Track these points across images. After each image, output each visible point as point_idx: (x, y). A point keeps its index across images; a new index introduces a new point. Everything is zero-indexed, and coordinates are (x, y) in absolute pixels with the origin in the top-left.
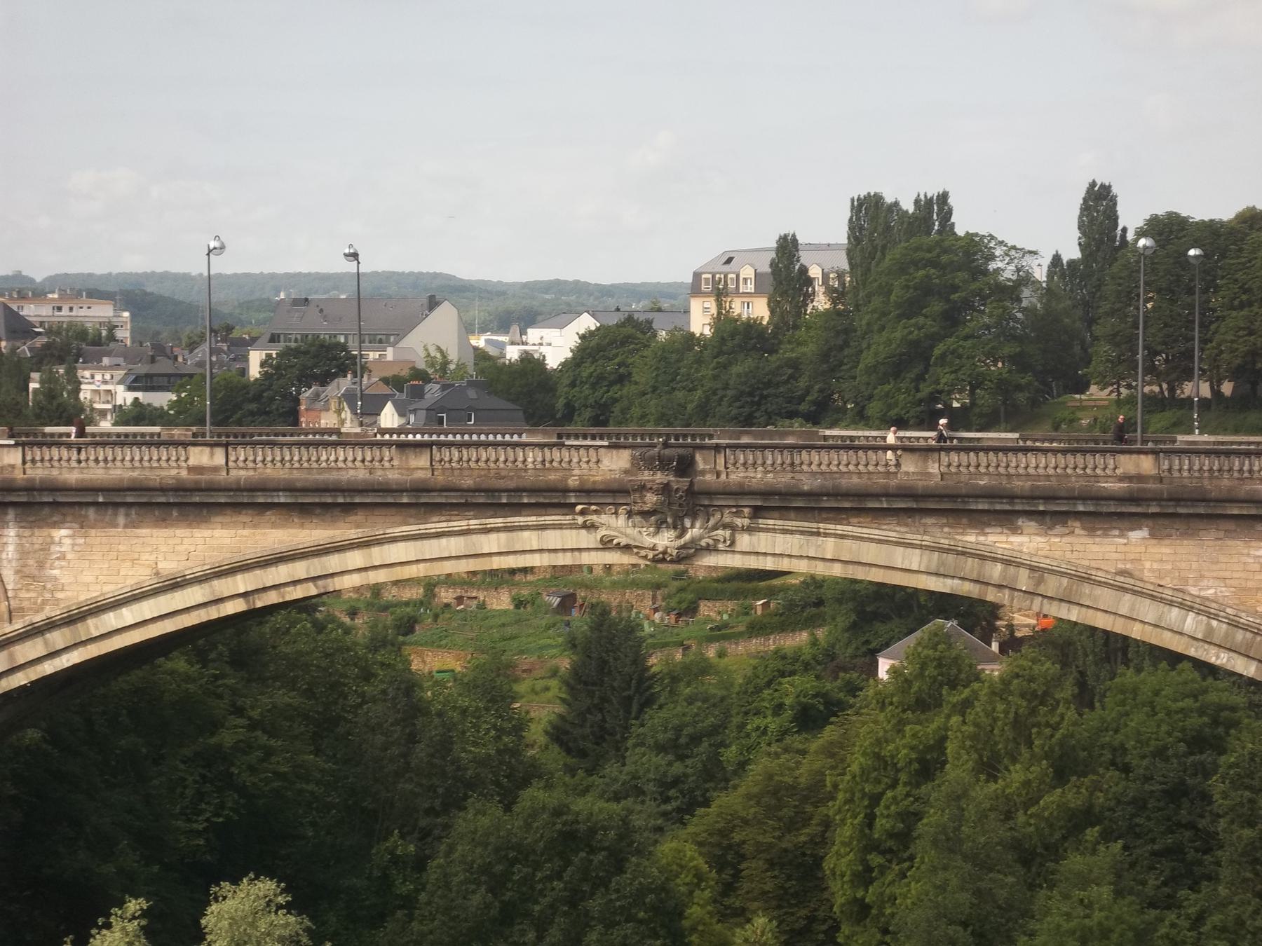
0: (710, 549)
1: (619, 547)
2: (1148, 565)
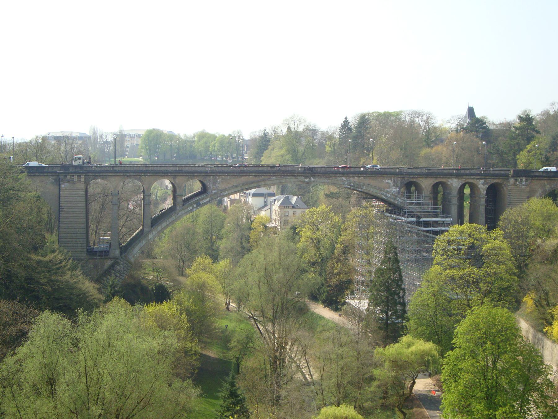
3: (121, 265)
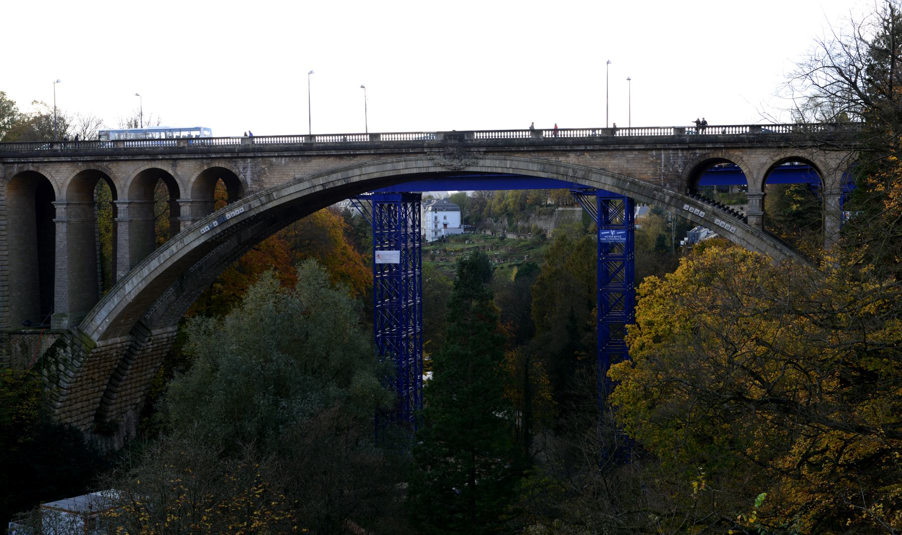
1: (441, 165)
2: (610, 166)
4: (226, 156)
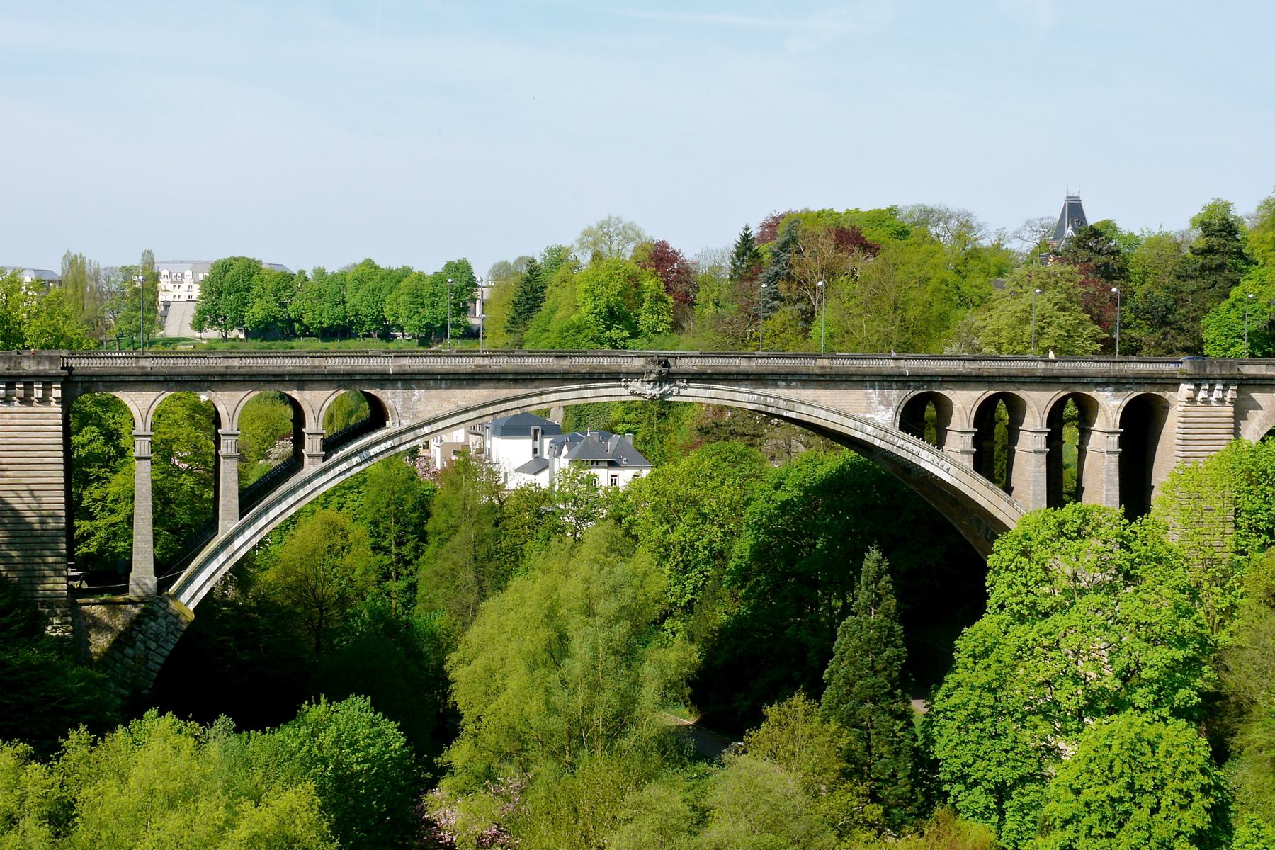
0: (671, 395)
3: (160, 619)
4: (374, 377)
